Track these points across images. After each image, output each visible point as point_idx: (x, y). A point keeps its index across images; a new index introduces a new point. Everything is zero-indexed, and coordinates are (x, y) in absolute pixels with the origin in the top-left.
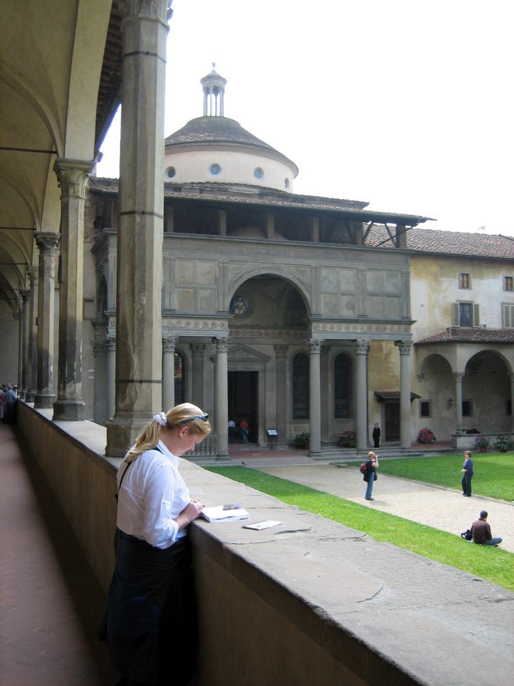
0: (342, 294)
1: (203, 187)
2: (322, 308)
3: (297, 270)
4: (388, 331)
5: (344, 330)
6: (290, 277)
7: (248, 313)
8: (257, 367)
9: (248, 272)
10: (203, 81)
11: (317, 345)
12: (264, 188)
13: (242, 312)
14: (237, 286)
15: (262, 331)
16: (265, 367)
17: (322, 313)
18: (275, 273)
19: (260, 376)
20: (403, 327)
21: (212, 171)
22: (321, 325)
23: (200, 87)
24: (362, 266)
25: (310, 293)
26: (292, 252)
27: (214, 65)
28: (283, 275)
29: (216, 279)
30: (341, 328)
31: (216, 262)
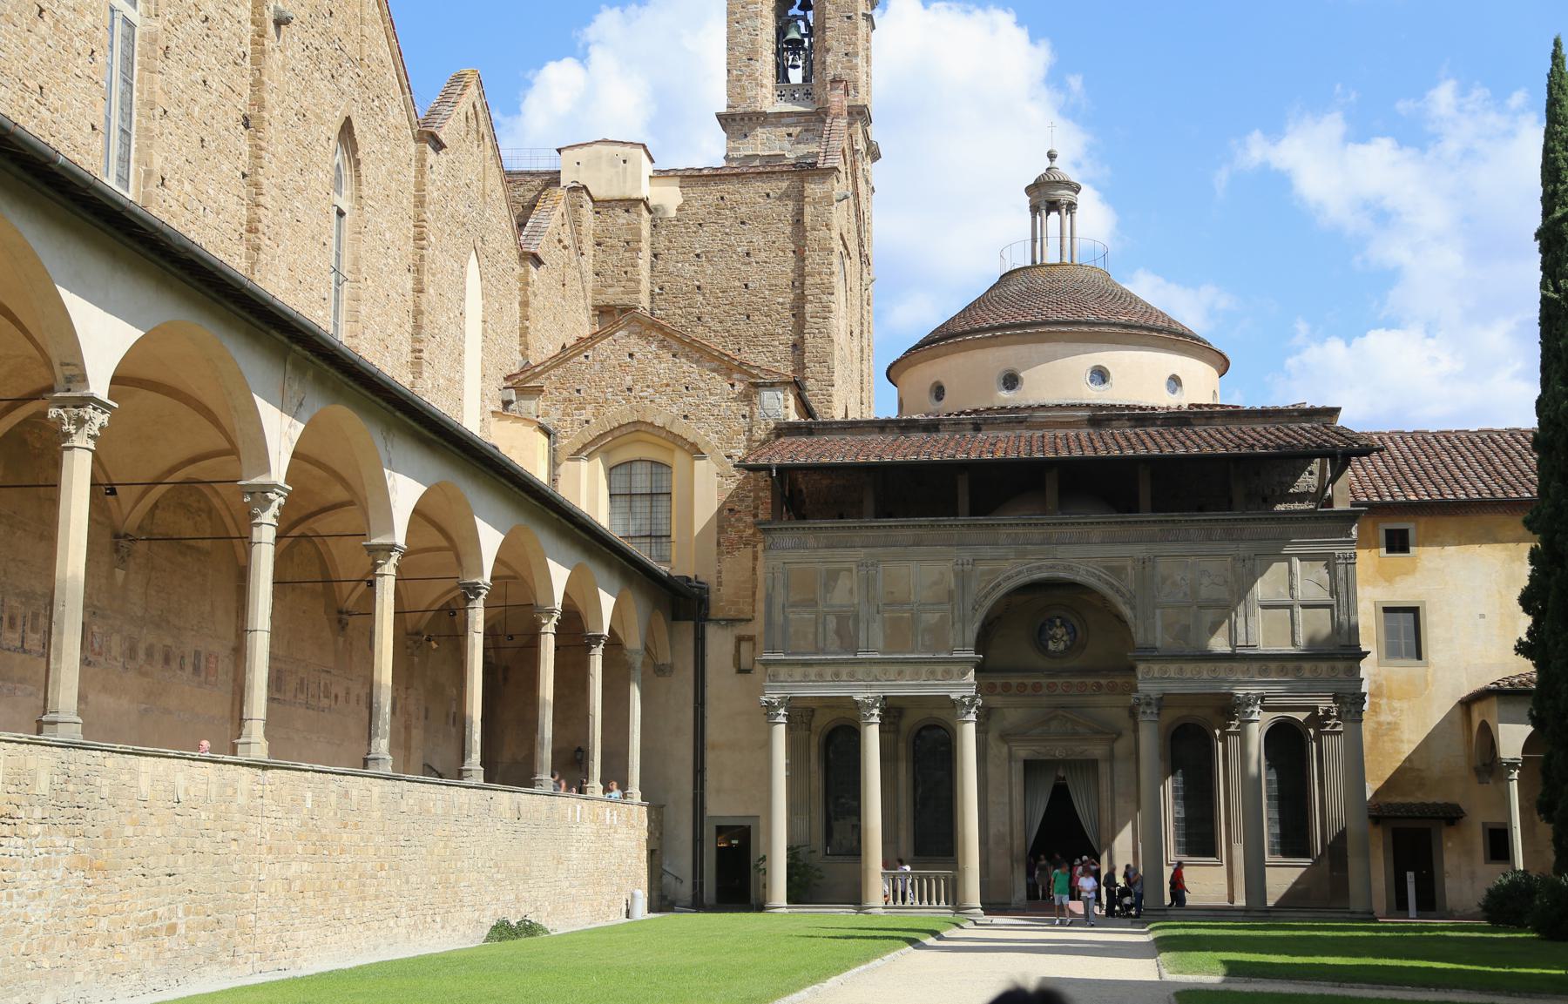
0: (1200, 607)
1: (980, 421)
2: (1158, 635)
3: (1105, 567)
4: (1307, 675)
5: (1205, 676)
6: (1092, 581)
7: (1074, 647)
8: (1097, 750)
9: (1009, 578)
10: (1029, 190)
11: (1148, 704)
12: (1101, 407)
13: (1062, 646)
14: (988, 603)
15: (1103, 681)
16: (1112, 750)
17: (1158, 644)
18: (1062, 574)
19: (1104, 768)
20: (1341, 665)
21: (1005, 384)
22: (1156, 668)
23: (1025, 201)
24: (1243, 549)
25: (1133, 608)
26: (1097, 533)
27: (1051, 156)
28: (1078, 579)
29: (950, 593)
30: (1199, 673)
31: (950, 564)
